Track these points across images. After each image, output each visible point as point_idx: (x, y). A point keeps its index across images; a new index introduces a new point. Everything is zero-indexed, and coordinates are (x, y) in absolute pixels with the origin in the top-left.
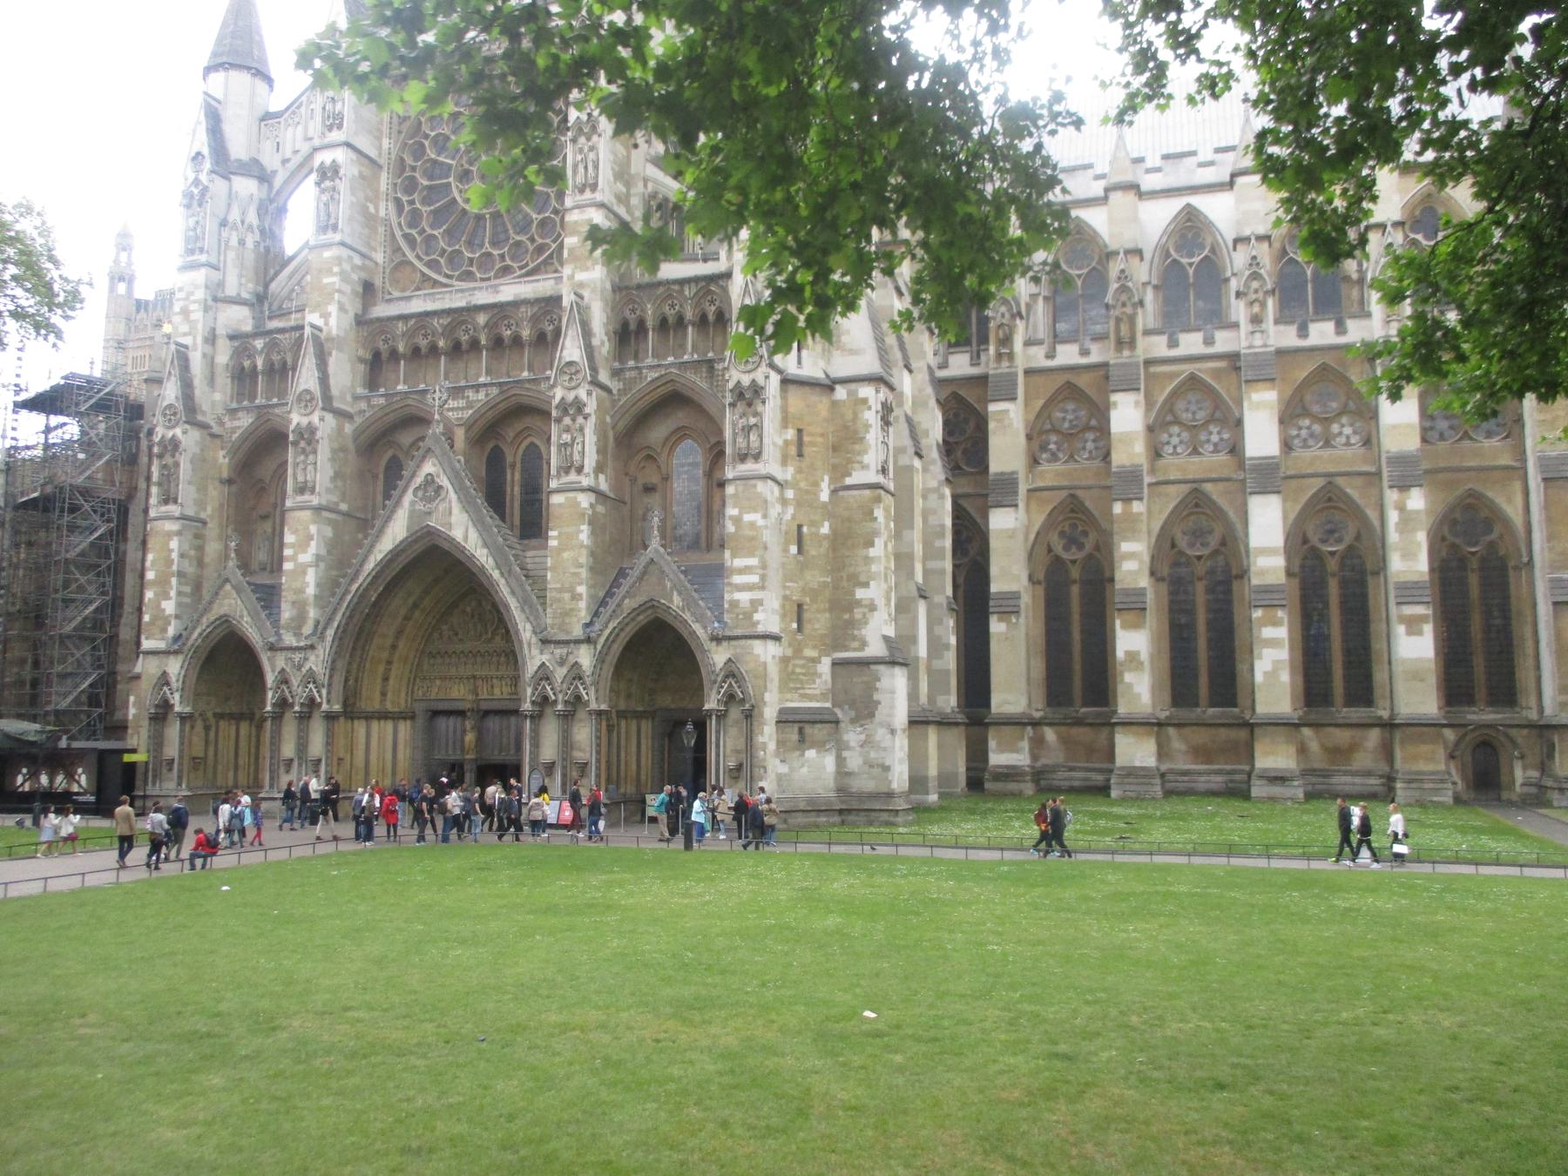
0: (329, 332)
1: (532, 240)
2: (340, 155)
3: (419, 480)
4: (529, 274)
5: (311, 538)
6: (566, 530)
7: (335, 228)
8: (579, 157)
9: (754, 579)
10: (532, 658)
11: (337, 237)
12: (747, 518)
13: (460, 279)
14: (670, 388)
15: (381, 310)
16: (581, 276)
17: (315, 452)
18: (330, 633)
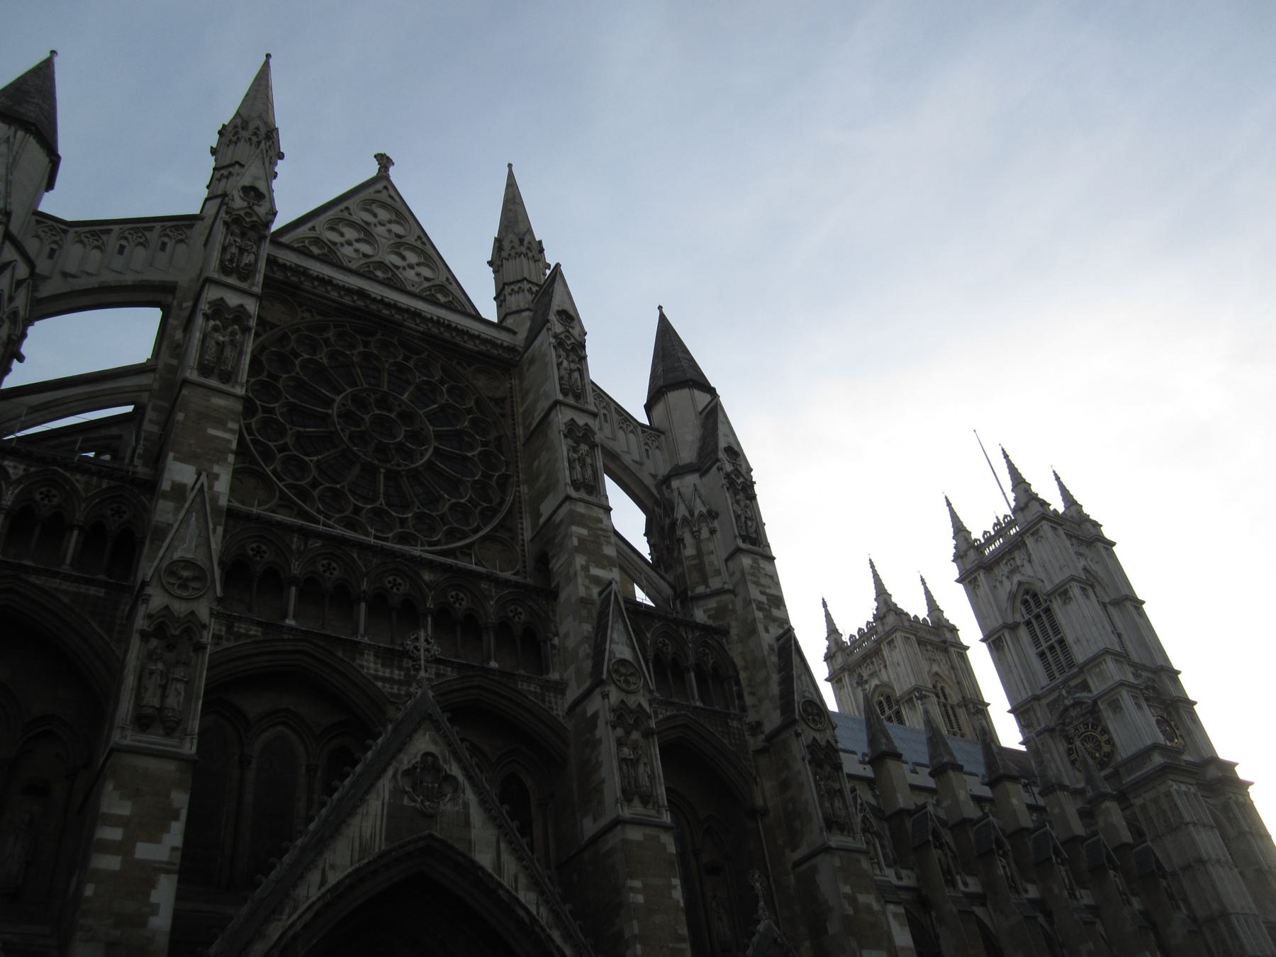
3: (407, 760)
5: (176, 817)
7: (227, 377)
11: (240, 391)
12: (863, 898)
13: (337, 521)
16: (595, 571)
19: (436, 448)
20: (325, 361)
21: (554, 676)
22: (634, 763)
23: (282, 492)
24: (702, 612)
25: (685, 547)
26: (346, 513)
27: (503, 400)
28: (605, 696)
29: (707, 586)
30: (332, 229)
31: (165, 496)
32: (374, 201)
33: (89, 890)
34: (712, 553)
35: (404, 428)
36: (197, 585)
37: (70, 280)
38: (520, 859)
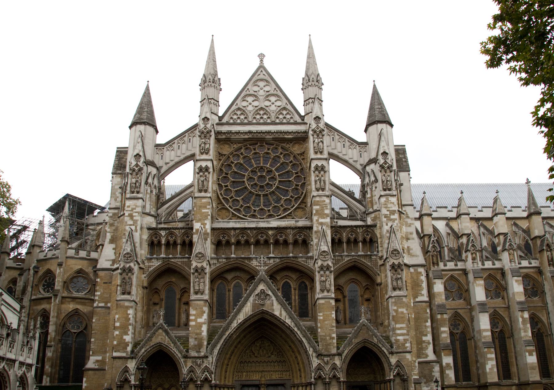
0: (206, 231)
1: (282, 206)
2: (209, 164)
3: (257, 291)
4: (281, 218)
5: (205, 313)
6: (326, 313)
7: (206, 191)
8: (318, 178)
9: (405, 332)
10: (314, 361)
11: (209, 195)
12: (400, 310)
14: (353, 264)
15: (222, 224)
16: (321, 220)
17: (203, 278)
18: (216, 351)
19: (279, 181)
20: (242, 162)
21: (310, 254)
22: (324, 282)
23: (232, 212)
24: (370, 218)
25: (367, 194)
26: (251, 213)
27: (304, 153)
28: (317, 263)
29: (373, 209)
30: (244, 100)
31: (195, 234)
32: (258, 80)
33: (190, 329)
34: (375, 196)
35: (268, 177)
36: (202, 258)
37: (168, 165)
38: (287, 312)
